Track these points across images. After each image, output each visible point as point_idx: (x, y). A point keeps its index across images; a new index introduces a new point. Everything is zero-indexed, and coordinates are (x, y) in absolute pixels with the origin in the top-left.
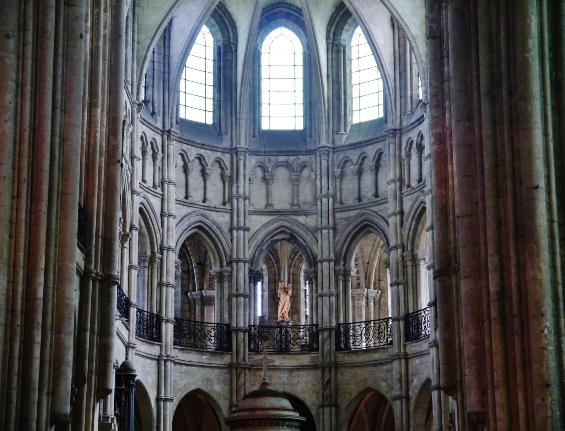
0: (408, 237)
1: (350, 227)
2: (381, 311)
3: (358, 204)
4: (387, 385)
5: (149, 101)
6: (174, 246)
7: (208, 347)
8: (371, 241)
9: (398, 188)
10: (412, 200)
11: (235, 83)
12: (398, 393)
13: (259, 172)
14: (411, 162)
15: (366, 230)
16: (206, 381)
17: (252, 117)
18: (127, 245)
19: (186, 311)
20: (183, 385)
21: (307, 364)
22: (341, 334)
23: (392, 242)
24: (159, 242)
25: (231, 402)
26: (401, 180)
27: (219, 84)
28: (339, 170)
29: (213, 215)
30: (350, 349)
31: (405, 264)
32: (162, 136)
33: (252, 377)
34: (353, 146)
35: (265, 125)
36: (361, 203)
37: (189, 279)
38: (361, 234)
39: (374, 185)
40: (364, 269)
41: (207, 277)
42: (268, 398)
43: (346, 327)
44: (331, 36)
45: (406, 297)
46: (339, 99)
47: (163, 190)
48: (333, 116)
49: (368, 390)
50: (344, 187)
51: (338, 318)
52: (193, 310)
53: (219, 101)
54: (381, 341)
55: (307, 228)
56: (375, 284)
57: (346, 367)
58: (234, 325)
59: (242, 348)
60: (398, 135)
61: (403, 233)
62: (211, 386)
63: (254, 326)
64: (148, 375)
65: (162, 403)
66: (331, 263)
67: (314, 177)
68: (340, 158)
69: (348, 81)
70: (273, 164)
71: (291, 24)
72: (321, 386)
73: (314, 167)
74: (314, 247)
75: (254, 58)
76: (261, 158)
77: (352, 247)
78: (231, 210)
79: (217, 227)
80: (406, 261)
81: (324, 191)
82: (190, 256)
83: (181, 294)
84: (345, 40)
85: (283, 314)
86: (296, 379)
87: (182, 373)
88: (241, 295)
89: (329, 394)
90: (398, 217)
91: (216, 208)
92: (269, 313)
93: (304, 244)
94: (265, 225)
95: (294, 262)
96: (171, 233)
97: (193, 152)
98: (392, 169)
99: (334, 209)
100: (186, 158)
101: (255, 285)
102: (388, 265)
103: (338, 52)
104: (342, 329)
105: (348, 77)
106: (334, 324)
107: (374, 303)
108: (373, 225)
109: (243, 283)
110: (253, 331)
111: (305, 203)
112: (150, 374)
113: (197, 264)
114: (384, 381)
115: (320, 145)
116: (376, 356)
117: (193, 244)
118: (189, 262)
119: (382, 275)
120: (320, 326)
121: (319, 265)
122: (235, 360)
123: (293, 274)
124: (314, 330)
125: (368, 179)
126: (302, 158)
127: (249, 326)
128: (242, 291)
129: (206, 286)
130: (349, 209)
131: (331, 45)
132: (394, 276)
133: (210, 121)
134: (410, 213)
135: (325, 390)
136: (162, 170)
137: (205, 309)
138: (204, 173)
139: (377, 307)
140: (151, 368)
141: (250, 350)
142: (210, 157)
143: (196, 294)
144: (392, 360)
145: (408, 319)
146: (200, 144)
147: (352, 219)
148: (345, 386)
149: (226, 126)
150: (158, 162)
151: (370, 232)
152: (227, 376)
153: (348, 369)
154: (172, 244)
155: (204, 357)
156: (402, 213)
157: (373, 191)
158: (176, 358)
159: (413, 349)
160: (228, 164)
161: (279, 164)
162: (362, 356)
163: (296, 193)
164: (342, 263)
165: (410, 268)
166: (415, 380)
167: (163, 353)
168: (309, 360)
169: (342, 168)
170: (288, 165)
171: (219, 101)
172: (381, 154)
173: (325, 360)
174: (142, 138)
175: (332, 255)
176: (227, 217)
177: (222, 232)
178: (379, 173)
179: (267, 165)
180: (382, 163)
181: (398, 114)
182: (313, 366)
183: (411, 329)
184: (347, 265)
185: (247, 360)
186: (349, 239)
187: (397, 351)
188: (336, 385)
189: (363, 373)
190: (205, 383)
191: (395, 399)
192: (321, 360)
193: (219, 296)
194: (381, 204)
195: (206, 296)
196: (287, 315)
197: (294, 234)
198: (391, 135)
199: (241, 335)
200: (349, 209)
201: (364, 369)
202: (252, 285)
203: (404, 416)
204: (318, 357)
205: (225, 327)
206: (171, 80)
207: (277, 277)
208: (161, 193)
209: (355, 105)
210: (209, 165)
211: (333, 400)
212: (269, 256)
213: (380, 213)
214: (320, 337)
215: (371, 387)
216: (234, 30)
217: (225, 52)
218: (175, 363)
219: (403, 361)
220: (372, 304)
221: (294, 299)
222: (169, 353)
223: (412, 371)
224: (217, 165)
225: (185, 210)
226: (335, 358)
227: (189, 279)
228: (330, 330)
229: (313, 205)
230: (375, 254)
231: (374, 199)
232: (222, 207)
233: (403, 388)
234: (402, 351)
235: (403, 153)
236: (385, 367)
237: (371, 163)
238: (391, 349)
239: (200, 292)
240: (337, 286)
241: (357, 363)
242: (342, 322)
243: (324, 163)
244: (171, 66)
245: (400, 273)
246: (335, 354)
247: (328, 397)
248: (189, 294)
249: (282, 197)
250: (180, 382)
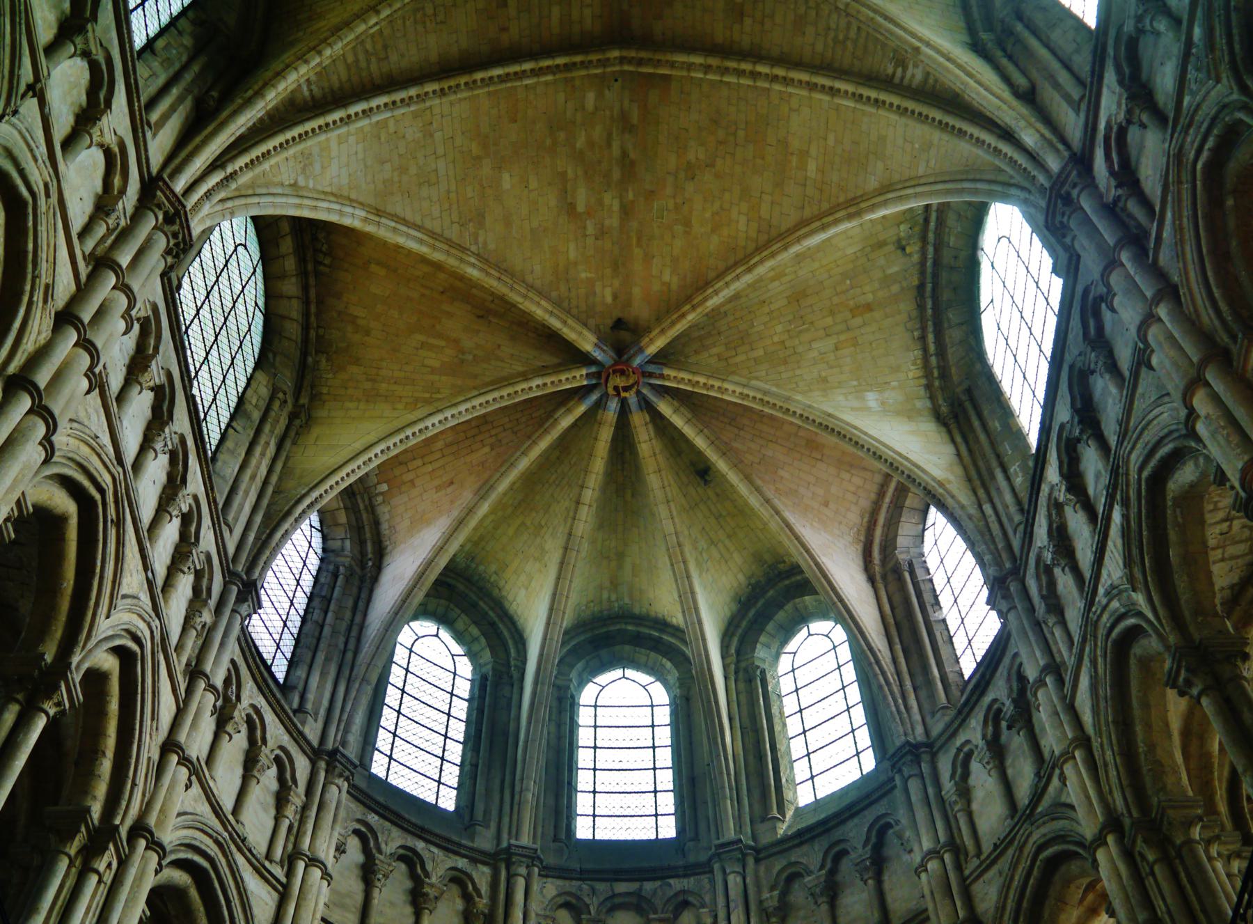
5: (295, 688)
9: (949, 867)
10: (1000, 873)
11: (516, 740)
14: (975, 806)
17: (551, 801)
18: (106, 862)
26: (955, 847)
28: (776, 893)
32: (313, 763)
34: (803, 836)
35: (583, 830)
39: (876, 903)
44: (733, 651)
46: (761, 757)
47: (290, 873)
48: (748, 790)
53: (475, 766)
60: (926, 757)
68: (778, 868)
69: (777, 728)
70: (602, 899)
71: (642, 654)
73: (707, 899)
75: (563, 711)
76: (572, 886)
84: (764, 661)
97: (392, 840)
98: (923, 831)
100: (372, 844)
103: (750, 681)
105: (776, 720)
115: (721, 841)
126: (677, 884)
131: (733, 667)
133: (448, 801)
134: (1004, 907)
136: (296, 833)
142: (439, 864)
146: (415, 825)
149: (487, 812)
150: (290, 812)
160: (484, 888)
161: (617, 900)
169: (784, 894)
171: (476, 766)
174: (249, 721)
178: (886, 877)
179: (587, 900)
181: (917, 717)
198: (909, 758)
206: (358, 662)
208: (284, 880)
209: (801, 771)
210: (434, 880)
216: (520, 646)
217: (496, 685)
224: (455, 889)
235: (948, 786)
237: (860, 851)
243: (734, 881)
244: (363, 640)
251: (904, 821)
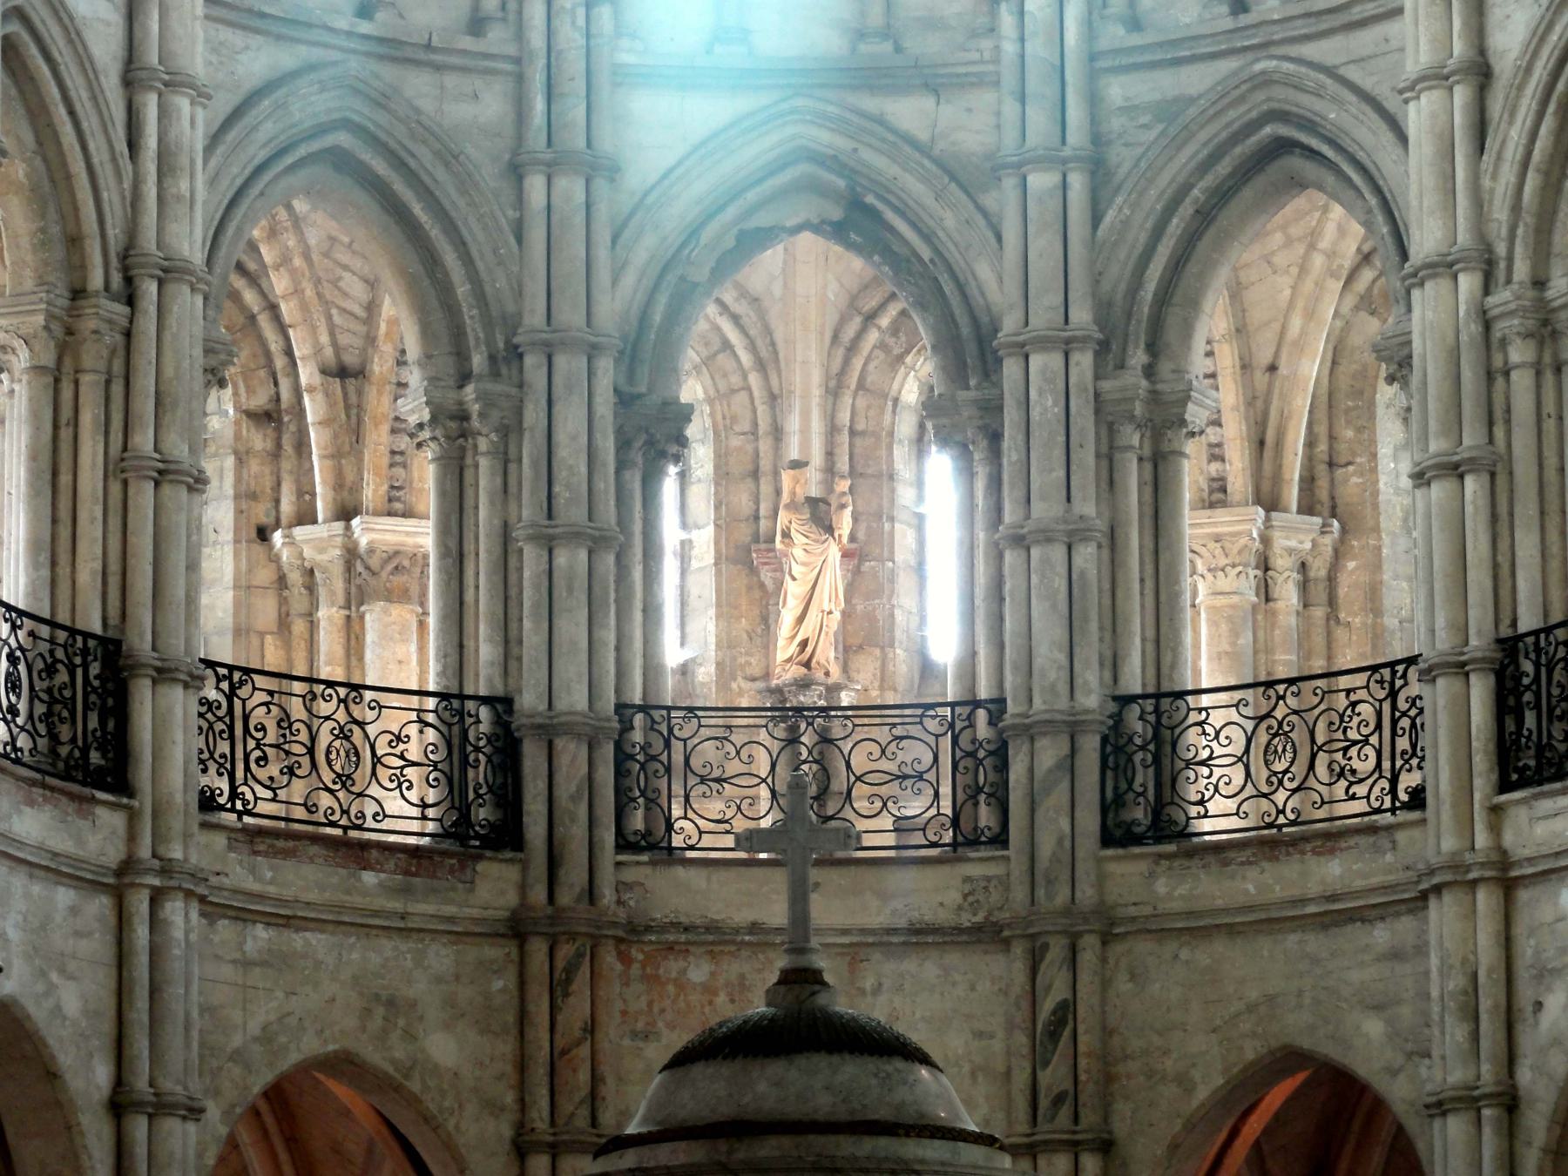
0: (1516, 208)
1: (1184, 156)
2: (1340, 633)
3: (1228, 23)
6: (198, 258)
7: (386, 824)
8: (1289, 243)
12: (1457, 1075)
16: (380, 1011)
19: (262, 635)
20: (254, 1027)
21: (944, 917)
22: (1138, 756)
23: (1426, 239)
24: (115, 233)
25: (521, 1127)
30: (1184, 834)
31: (1498, 361)
33: (637, 987)
36: (1244, 20)
37: (276, 454)
38: (1247, 193)
40: (1250, 402)
41: (378, 440)
42: (821, 1061)
43: (1157, 711)
45: (1504, 545)
49: (1288, 1059)
51: (1114, 665)
52: (299, 627)
54: (1360, 790)
55: (935, 161)
56: (1308, 481)
57: (1163, 934)
59: (575, 833)
61: (1486, 182)
62: (410, 1036)
63: (644, 709)
64: (62, 971)
65: (139, 1127)
66: (1075, 357)
72: (1022, 1039)
74: (984, 271)
77: (1193, 267)
78: (518, 61)
79: (437, 154)
80: (1504, 342)
82: (282, 329)
83: (237, 541)
85: (804, 644)
86: (883, 999)
87: (246, 964)
88: (575, 536)
89: (1067, 1085)
90: (1462, 95)
91: (428, 46)
92: (718, 646)
93: (926, 253)
95: (857, 363)
96: (184, 186)
99: (1093, 57)
101: (650, 481)
102: (1400, 365)
104: (1139, 727)
106: (1091, 700)
107: (1304, 586)
108: (1314, 143)
109: (584, 469)
110: (637, 736)
111: (932, 23)
112: (72, 966)
113: (324, 372)
114: (1378, 1008)
116: (1332, 872)
117: (298, 262)
118: (280, 362)
119: (1350, 433)
120: (1011, 707)
121: (1011, 369)
122: (539, 894)
123: (853, 432)
124: (983, 730)
127: (621, 707)
128: (572, 512)
129: (372, 491)
132: (1433, 425)
134: (1528, 70)
135: (1046, 1064)
137: (368, 617)
139: (1319, 613)
140: (78, 934)
141: (625, 844)
143: (315, 542)
144: (1424, 896)
145: (1518, 666)
147: (1193, 111)
148: (1157, 1041)
151: (1298, 184)
152: (498, 984)
153: (1171, 946)
154: (190, 243)
155: (369, 878)
156: (1481, 72)
158: (214, 880)
159: (1541, 830)
162: (1252, 872)
164: (1139, 357)
165: (1522, 381)
167: (145, 852)
168: (954, 897)
173: (1041, 893)
175: (1082, 315)
176: (491, 105)
177: (466, 183)
182: (977, 929)
183: (1530, 719)
184: (1165, 368)
185: (607, 896)
186: (1176, 226)
187: (1449, 844)
188: (1107, 1032)
189: (1256, 970)
190: (377, 1022)
191: (1439, 1108)
192: (1019, 894)
193: (453, 544)
194: (1363, 23)
195: (371, 551)
196: (827, 654)
197: (870, 199)
199: (571, 755)
201: (1265, 945)
202: (634, 480)
204: (1005, 883)
205: (484, 713)
207: (765, 446)
211: (1089, 1118)
212: (718, 329)
213: (1353, 73)
214: (1017, 771)
215: (1306, 1043)
218: (212, 910)
219: (1486, 899)
220: (1288, 594)
221: (857, 572)
222: (177, 854)
223: (1537, 953)
226: (1101, 880)
227: (276, 454)
228: (1073, 728)
229: (974, 34)
230: (1310, 315)
232: (467, 43)
233: (1485, 1044)
234: (1482, 839)
236: (1381, 935)
238: (1416, 833)
239: (338, 526)
240: (1110, 482)
241: (1225, 911)
242: (1138, 690)
246: (1100, 861)
247: (1059, 1100)
248: (278, 537)
250: (237, 1016)
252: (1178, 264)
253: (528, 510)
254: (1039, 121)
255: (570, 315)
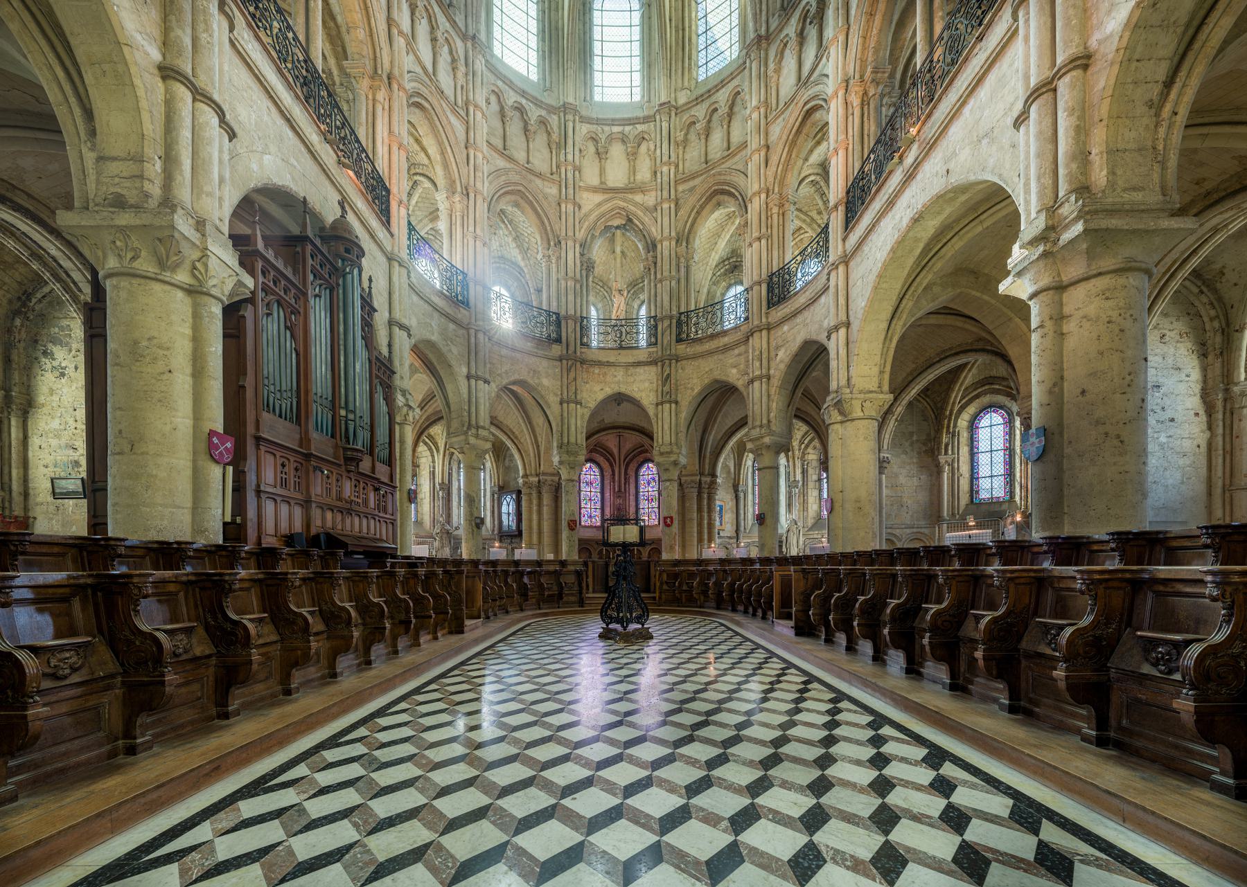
4: (739, 371)
12: (757, 373)
13: (592, 149)
15: (714, 201)
27: (544, 31)
29: (538, 182)
50: (687, 156)
58: (563, 313)
67: (652, 148)
74: (653, 230)
76: (593, 128)
81: (665, 158)
94: (599, 205)
121: (659, 247)
125: (717, 138)
126: (640, 128)
128: (571, 274)
130: (693, 176)
138: (526, 130)
157: (725, 145)
160: (556, 129)
163: (633, 171)
165: (775, 217)
166: (781, 354)
170: (624, 140)
172: (738, 93)
175: (673, 234)
180: (736, 109)
187: (756, 323)
200: (693, 176)
202: (584, 273)
203: (765, 399)
214: (660, 328)
225: (501, 163)
228: (671, 318)
231: (726, 153)
234: (764, 320)
236: (736, 351)
245: (763, 225)
249: (617, 174)
251: (746, 90)
252: (692, 225)
253: (563, 273)
254: (665, 194)
255: (570, 233)
